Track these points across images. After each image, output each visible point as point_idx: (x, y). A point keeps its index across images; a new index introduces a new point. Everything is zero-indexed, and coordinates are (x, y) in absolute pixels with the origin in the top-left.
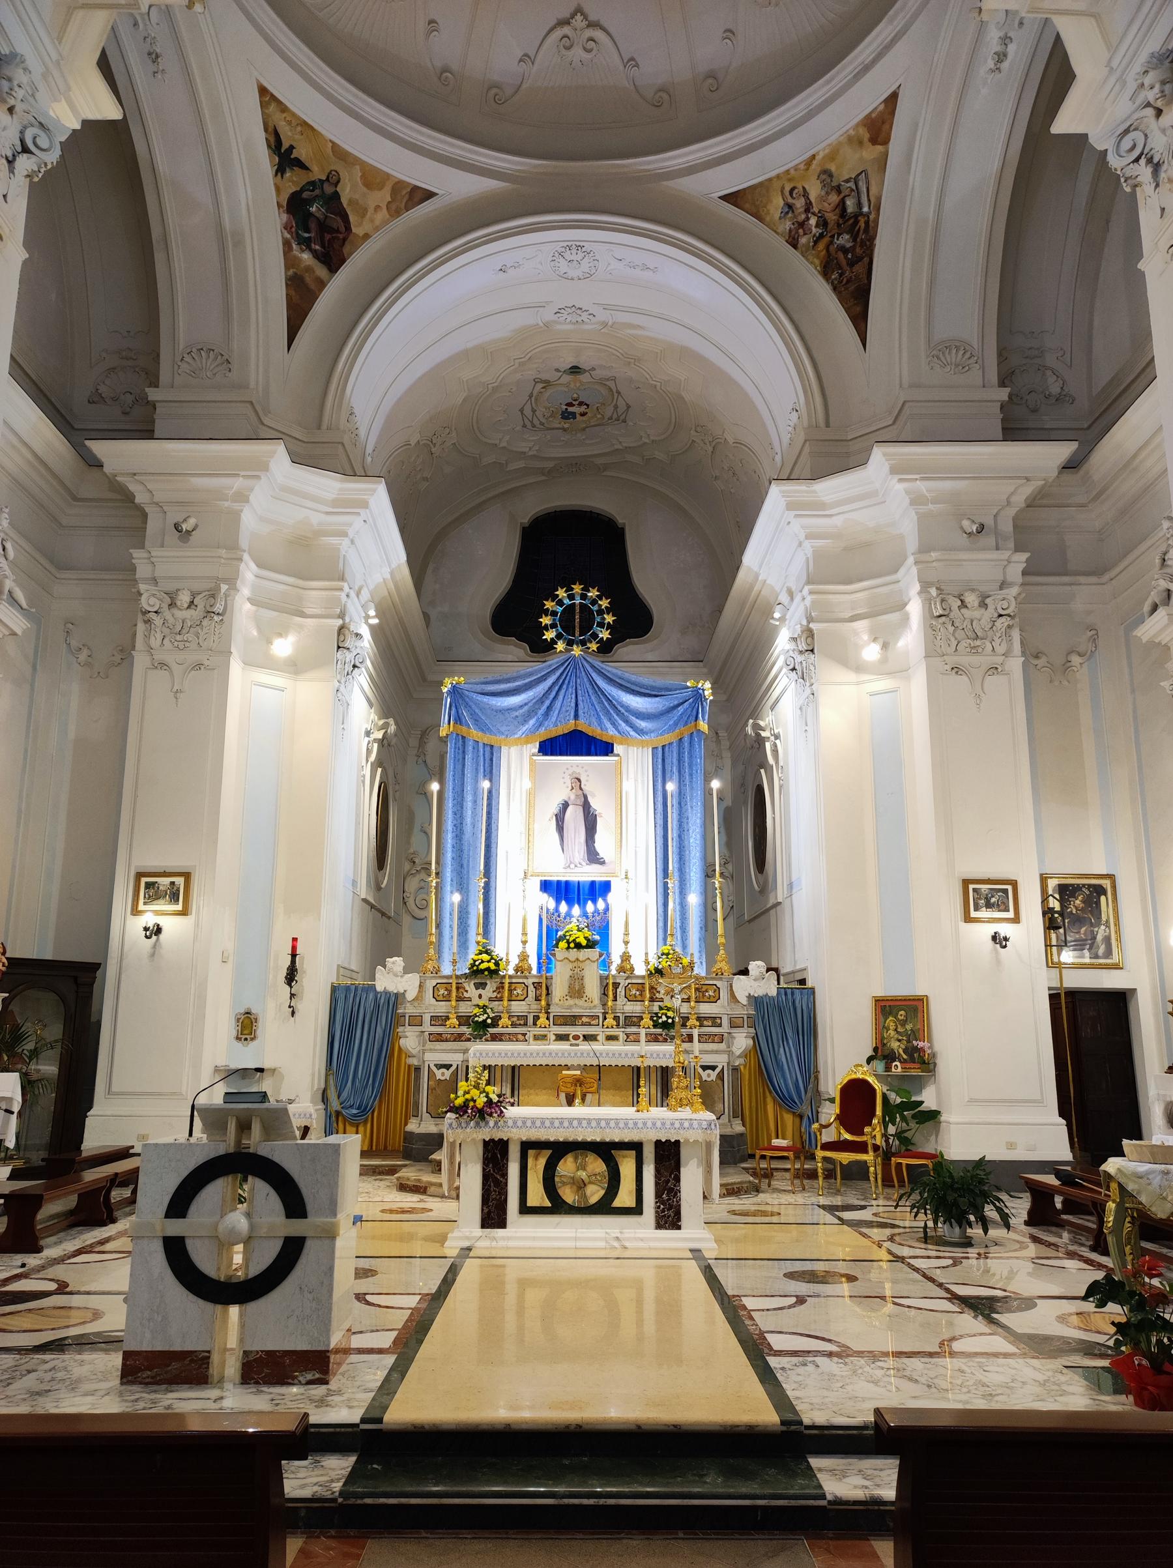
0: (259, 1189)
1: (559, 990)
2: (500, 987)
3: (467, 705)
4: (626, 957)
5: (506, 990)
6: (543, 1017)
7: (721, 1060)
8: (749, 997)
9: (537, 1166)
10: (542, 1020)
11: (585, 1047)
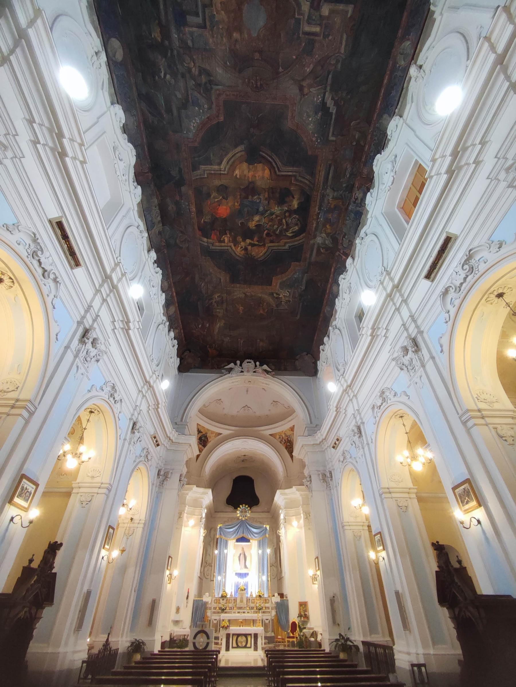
0: (204, 635)
1: (238, 601)
2: (227, 600)
3: (223, 531)
4: (251, 593)
5: (228, 601)
6: (235, 607)
7: (269, 618)
8: (275, 602)
9: (235, 638)
10: (235, 608)
11: (243, 615)
